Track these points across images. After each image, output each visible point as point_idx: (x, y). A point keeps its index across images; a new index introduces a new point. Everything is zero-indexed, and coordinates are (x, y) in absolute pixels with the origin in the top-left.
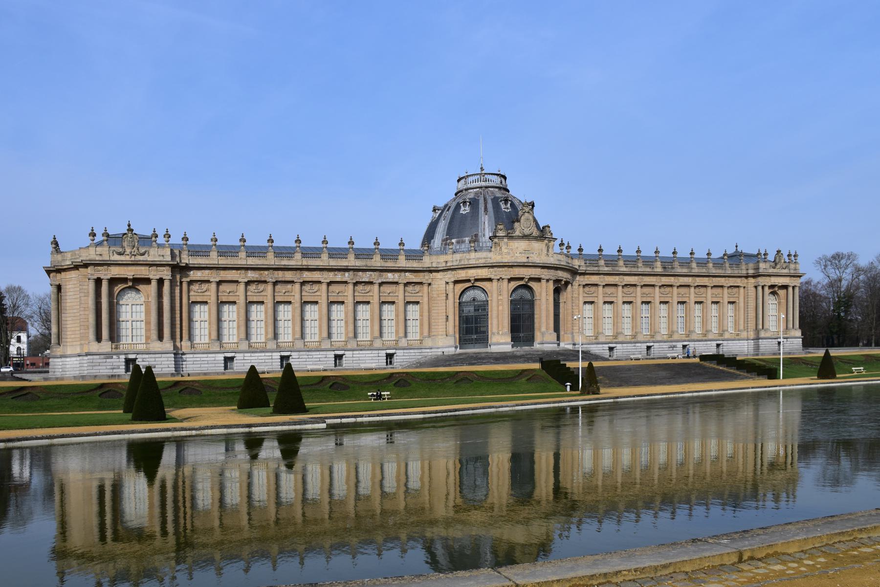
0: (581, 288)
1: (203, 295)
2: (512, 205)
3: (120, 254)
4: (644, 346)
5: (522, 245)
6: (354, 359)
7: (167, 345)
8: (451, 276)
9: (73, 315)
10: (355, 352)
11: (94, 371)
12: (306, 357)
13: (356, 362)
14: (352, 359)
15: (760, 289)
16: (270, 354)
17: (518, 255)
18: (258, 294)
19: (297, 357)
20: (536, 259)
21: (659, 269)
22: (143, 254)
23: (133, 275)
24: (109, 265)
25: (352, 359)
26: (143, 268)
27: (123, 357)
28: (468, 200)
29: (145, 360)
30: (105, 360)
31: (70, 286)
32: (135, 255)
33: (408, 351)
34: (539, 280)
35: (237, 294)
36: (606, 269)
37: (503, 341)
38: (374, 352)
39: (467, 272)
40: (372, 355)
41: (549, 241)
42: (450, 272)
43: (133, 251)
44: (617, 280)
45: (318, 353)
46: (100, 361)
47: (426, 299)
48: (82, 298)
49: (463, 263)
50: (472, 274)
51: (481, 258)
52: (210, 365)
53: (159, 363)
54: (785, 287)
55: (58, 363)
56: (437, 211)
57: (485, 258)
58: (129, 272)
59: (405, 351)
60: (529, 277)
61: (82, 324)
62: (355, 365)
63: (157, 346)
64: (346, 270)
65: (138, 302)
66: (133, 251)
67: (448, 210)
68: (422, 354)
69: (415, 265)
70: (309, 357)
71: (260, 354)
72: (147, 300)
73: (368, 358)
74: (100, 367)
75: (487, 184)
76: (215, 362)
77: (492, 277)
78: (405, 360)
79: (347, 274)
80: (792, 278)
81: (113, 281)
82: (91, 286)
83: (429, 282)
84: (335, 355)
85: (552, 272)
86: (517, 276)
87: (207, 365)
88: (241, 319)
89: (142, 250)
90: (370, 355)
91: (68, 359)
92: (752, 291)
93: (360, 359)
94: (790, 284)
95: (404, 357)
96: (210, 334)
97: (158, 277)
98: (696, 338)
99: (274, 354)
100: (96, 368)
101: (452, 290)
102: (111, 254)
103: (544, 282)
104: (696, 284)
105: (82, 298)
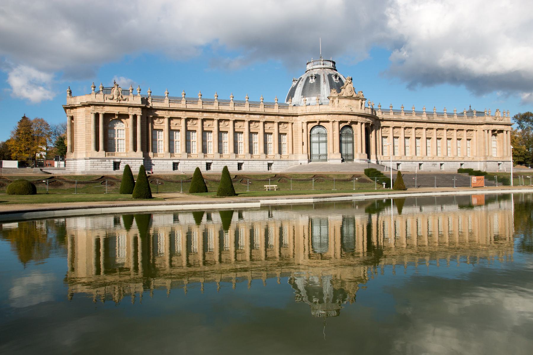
1: (160, 126)
2: (340, 79)
3: (111, 99)
4: (418, 163)
5: (347, 102)
6: (249, 165)
7: (139, 154)
8: (305, 119)
9: (81, 134)
10: (250, 162)
11: (95, 168)
12: (221, 164)
13: (250, 167)
14: (248, 165)
15: (486, 131)
16: (200, 161)
17: (344, 108)
18: (193, 126)
19: (216, 163)
20: (355, 111)
21: (425, 118)
22: (125, 100)
23: (119, 112)
24: (104, 105)
25: (248, 165)
26: (124, 108)
27: (112, 161)
28: (314, 75)
29: (125, 163)
30: (101, 162)
31: (79, 117)
32: (120, 100)
33: (280, 162)
34: (356, 123)
35: (181, 125)
36: (395, 117)
37: (336, 158)
38: (261, 162)
39: (315, 117)
40: (260, 164)
41: (362, 100)
42: (304, 116)
43: (118, 97)
44: (401, 124)
45: (228, 161)
46: (98, 162)
47: (290, 133)
48: (87, 125)
49: (312, 111)
50: (318, 118)
51: (323, 109)
52: (164, 167)
53: (135, 165)
54: (501, 131)
55: (71, 164)
56: (295, 81)
57: (325, 109)
58: (116, 110)
59: (279, 162)
60: (351, 121)
61: (87, 140)
62: (250, 169)
63: (133, 155)
65: (122, 128)
66: (118, 97)
67: (302, 81)
68: (288, 164)
70: (223, 163)
71: (194, 161)
72: (127, 127)
73: (257, 166)
74: (98, 167)
75: (324, 66)
76: (168, 165)
77: (330, 120)
78: (279, 167)
79: (244, 115)
80: (506, 126)
81: (106, 116)
82: (92, 118)
83: (292, 122)
84: (238, 163)
85: (364, 119)
86: (344, 120)
87: (163, 167)
88: (182, 140)
89: (124, 98)
90: (258, 164)
91: (78, 161)
93: (253, 165)
95: (278, 166)
96: (164, 148)
97: (134, 114)
98: (448, 160)
99: (202, 161)
100: (96, 167)
101: (306, 127)
102: (105, 99)
103: (359, 124)
104: (448, 128)
105: (87, 125)
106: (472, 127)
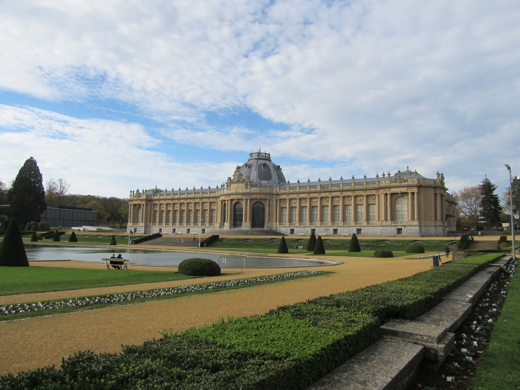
0: (278, 201)
20: (240, 191)
36: (290, 191)
54: (407, 193)
64: (190, 198)
69: (212, 195)
92: (382, 197)
94: (408, 192)
106: (374, 192)
